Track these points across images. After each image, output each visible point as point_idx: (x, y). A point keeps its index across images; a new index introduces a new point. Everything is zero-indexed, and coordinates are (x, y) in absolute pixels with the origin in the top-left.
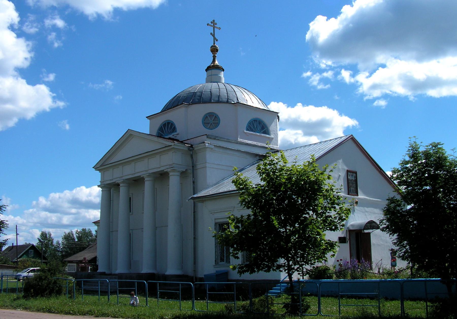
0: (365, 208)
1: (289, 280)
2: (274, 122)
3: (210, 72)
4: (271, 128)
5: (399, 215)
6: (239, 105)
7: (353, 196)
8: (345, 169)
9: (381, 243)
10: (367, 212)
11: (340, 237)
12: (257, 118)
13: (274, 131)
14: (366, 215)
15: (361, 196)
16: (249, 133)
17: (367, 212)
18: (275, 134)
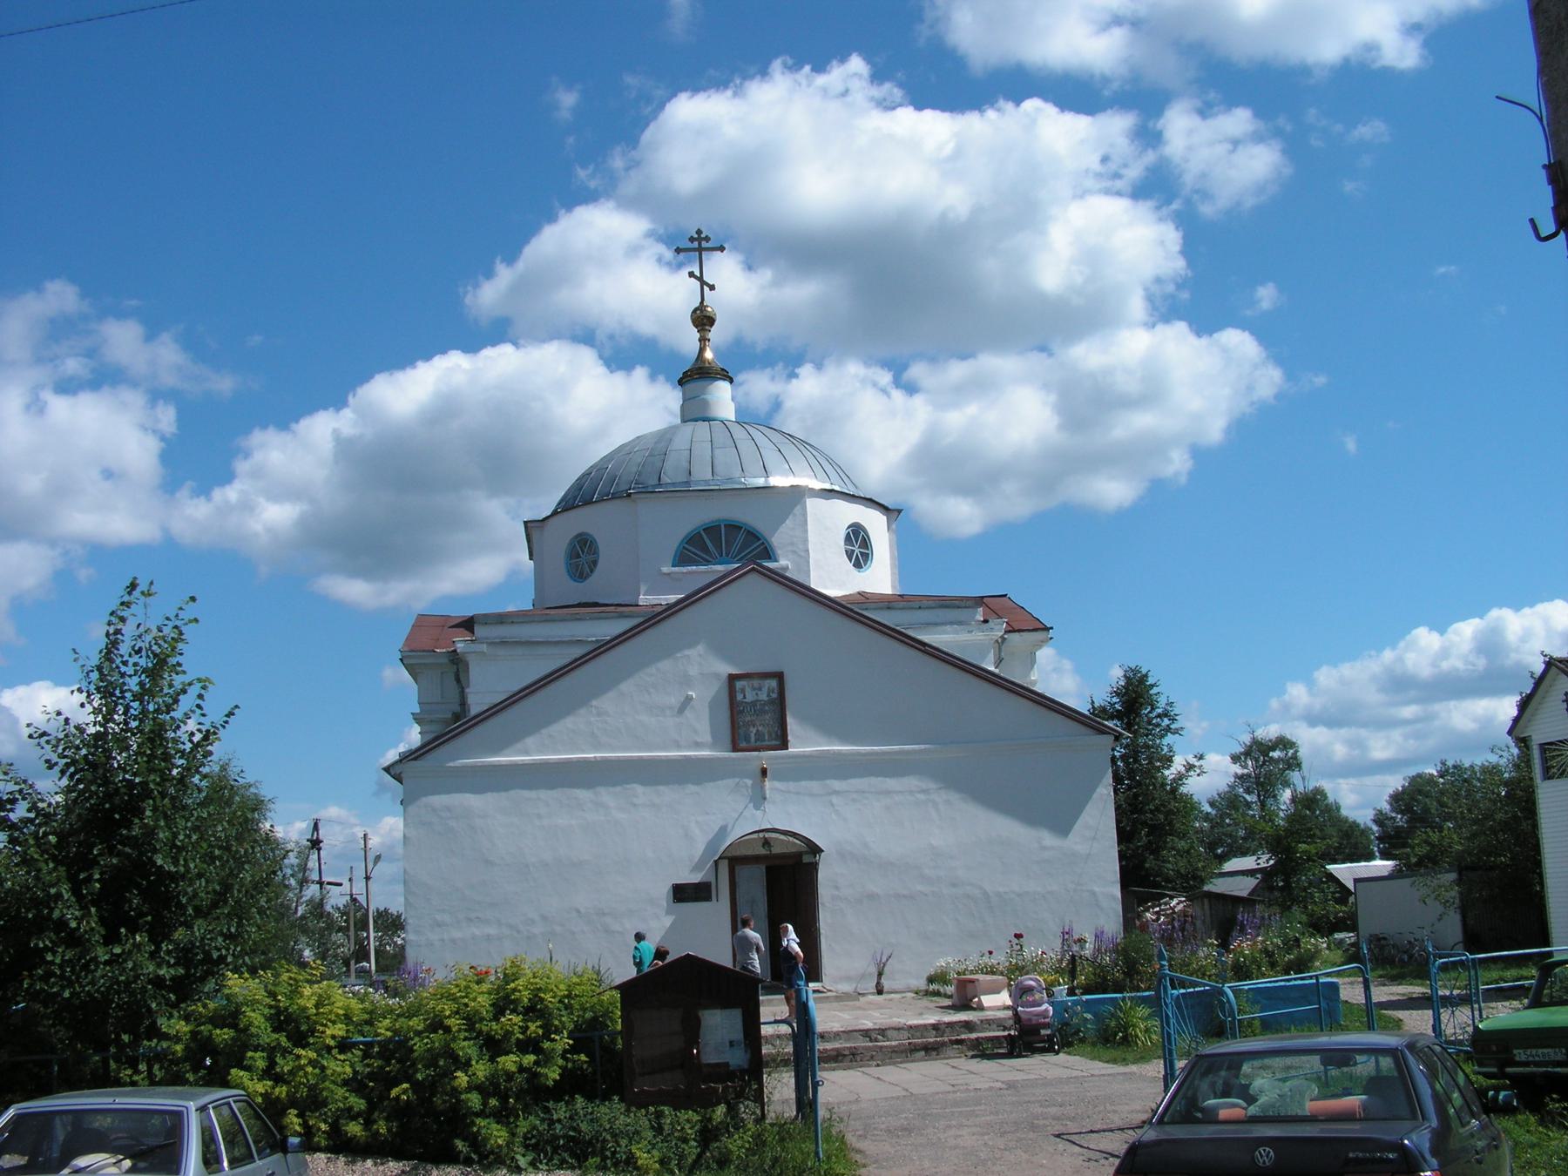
0: (828, 782)
1: (761, 998)
2: (791, 517)
3: (690, 386)
4: (777, 540)
5: (81, 877)
6: (640, 498)
7: (756, 753)
8: (717, 675)
9: (919, 888)
10: (836, 793)
11: (676, 884)
12: (719, 520)
13: (792, 544)
14: (832, 805)
15: (804, 742)
16: (683, 573)
17: (836, 793)
18: (794, 552)
